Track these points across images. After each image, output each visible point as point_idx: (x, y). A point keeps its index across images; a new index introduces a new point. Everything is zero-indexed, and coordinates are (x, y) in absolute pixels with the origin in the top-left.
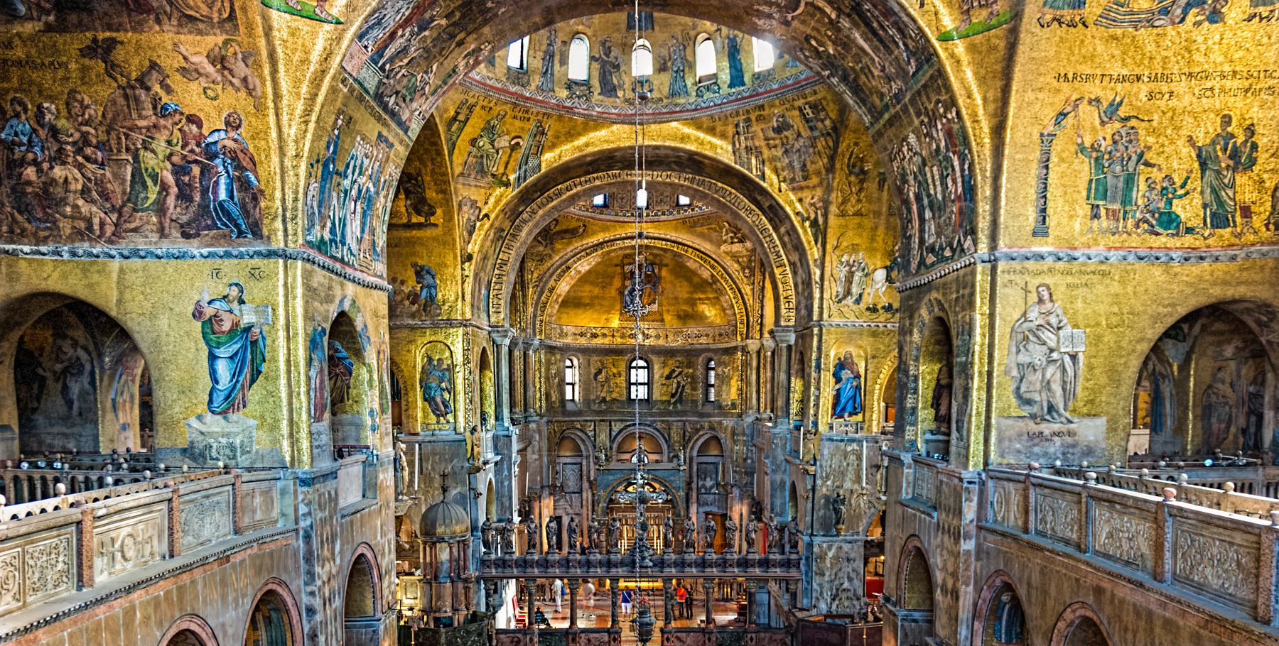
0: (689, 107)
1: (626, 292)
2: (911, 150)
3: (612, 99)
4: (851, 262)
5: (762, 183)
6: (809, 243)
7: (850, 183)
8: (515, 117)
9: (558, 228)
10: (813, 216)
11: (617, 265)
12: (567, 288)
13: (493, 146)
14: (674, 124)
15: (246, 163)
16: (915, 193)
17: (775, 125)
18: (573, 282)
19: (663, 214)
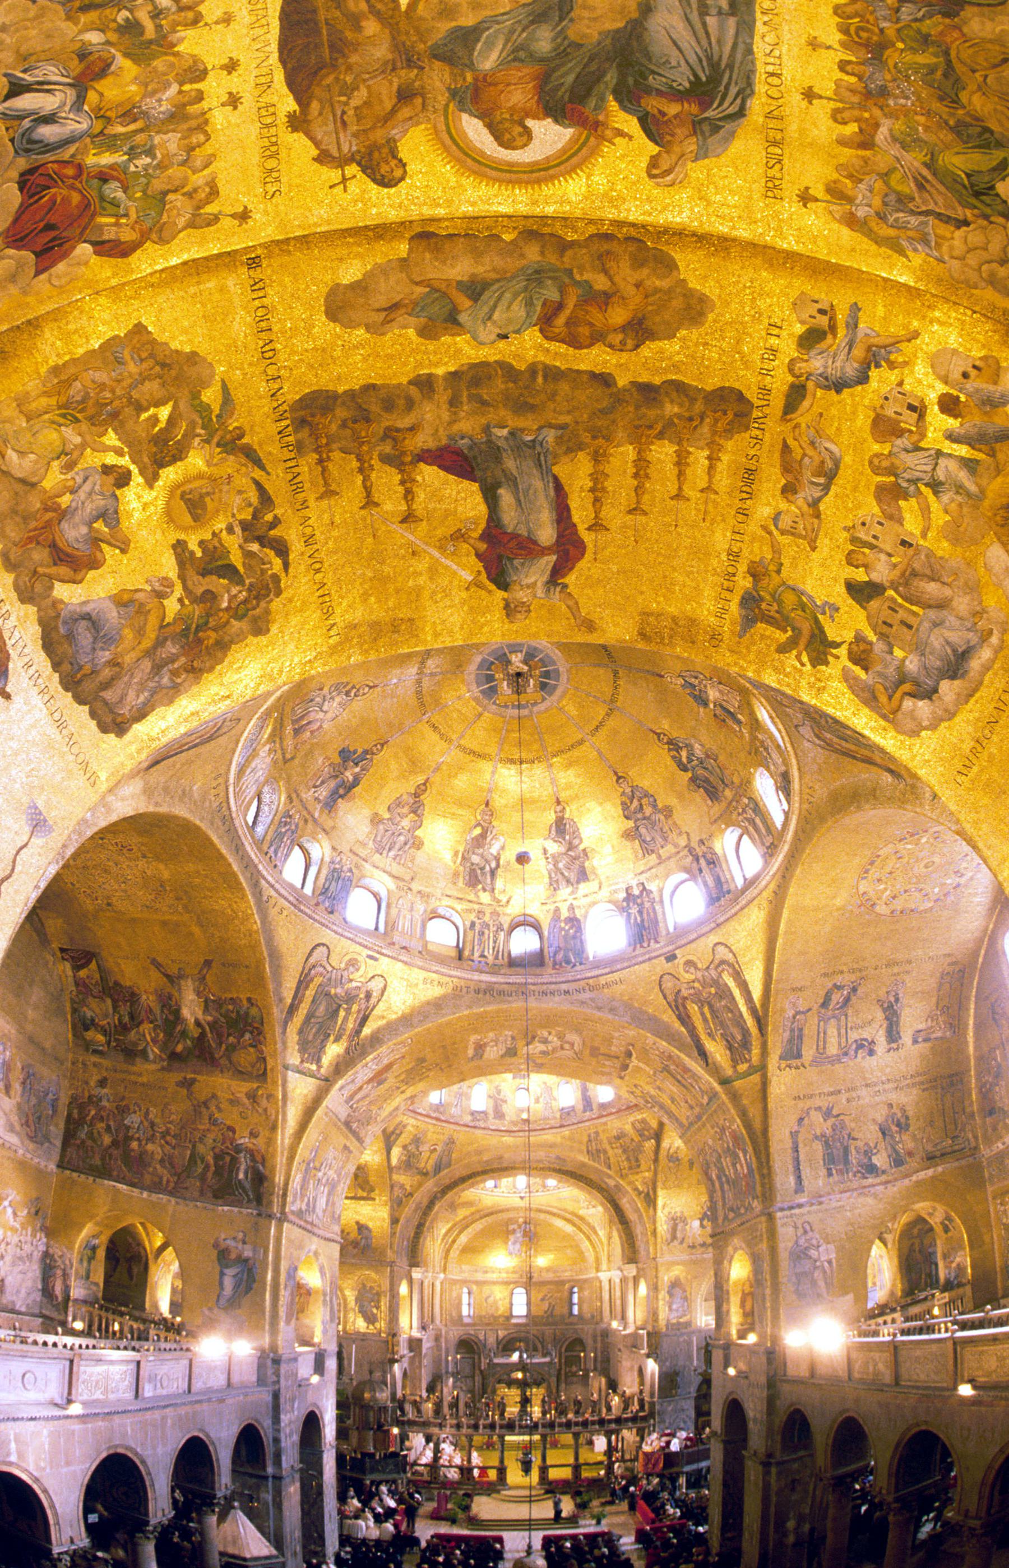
9: (461, 1200)
15: (259, 1158)
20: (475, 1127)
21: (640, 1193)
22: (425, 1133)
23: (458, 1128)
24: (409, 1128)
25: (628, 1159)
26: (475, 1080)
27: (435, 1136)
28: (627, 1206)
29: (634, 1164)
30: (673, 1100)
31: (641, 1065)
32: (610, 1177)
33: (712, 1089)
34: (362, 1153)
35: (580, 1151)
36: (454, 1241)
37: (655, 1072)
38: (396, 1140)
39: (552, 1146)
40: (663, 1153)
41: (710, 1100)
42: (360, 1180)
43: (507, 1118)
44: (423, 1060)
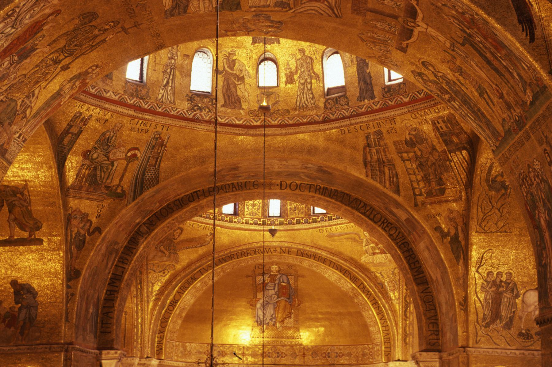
0: (317, 119)
1: (258, 305)
2: (538, 177)
3: (236, 111)
4: (498, 282)
5: (396, 197)
6: (450, 261)
7: (490, 199)
8: (132, 129)
9: (183, 237)
10: (453, 232)
11: (248, 276)
12: (192, 301)
13: (108, 158)
14: (301, 136)
16: (546, 221)
17: (408, 137)
18: (198, 295)
19: (298, 222)
20: (195, 120)
21: (444, 235)
22: (117, 130)
23: (169, 121)
24: (92, 123)
25: (426, 179)
26: (195, 44)
27: (133, 134)
28: (426, 254)
29: (435, 186)
30: (482, 92)
31: (432, 31)
32: (398, 205)
33: (539, 79)
34: (6, 169)
35: (353, 161)
36: (174, 303)
37: (453, 45)
38: (73, 142)
39: (311, 150)
40: (480, 174)
41: (536, 97)
42: (17, 210)
43: (245, 106)
44: (93, 15)
